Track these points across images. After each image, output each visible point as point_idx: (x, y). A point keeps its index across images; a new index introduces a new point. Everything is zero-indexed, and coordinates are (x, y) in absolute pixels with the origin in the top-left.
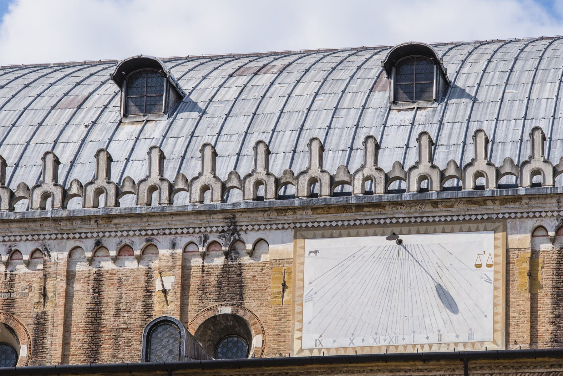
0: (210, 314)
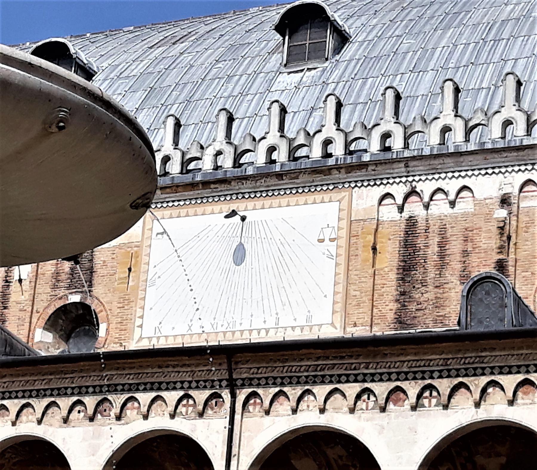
0: (60, 304)
